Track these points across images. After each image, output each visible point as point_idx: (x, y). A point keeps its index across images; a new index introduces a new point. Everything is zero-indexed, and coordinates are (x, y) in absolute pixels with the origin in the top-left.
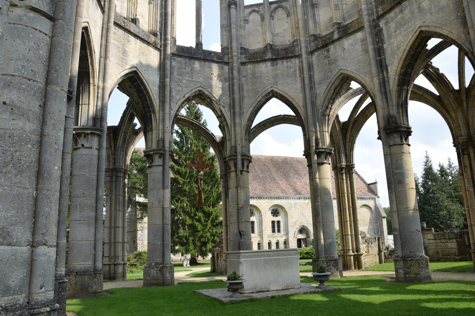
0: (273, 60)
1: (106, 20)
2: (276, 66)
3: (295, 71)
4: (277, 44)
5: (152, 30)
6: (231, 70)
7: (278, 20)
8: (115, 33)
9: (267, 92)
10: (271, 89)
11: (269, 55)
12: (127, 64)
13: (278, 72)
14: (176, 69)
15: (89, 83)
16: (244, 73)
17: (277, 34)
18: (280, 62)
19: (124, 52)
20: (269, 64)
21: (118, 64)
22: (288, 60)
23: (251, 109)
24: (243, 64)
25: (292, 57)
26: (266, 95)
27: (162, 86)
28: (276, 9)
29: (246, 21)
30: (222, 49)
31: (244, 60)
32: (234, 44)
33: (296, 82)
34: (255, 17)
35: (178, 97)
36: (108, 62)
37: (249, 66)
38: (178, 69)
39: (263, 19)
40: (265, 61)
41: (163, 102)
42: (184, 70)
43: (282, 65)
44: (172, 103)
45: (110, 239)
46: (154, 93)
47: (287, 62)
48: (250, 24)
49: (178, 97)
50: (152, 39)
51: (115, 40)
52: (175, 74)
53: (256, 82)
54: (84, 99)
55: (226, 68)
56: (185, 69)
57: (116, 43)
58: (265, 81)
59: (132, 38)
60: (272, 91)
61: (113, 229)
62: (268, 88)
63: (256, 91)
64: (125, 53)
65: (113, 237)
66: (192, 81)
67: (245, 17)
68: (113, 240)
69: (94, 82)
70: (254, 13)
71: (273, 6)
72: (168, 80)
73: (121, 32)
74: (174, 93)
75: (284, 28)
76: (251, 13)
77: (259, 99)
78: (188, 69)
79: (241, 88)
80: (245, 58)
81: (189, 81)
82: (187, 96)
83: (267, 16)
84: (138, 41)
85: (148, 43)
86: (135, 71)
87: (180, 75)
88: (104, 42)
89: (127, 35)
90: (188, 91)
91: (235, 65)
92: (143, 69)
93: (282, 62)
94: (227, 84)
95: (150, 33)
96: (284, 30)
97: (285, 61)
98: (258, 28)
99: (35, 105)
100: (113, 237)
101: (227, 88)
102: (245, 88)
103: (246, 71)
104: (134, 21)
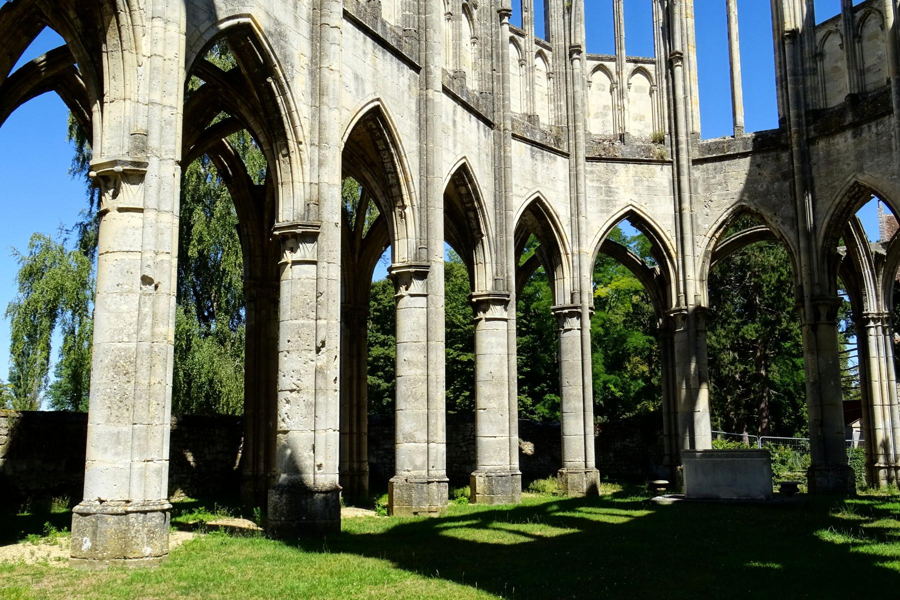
0: (856, 127)
1: (573, 164)
2: (861, 135)
3: (890, 140)
4: (869, 88)
5: (655, 134)
7: (869, 40)
8: (592, 172)
9: (847, 187)
10: (854, 180)
11: (849, 118)
12: (615, 206)
13: (865, 146)
14: (700, 182)
15: (560, 253)
16: (814, 159)
17: (869, 69)
18: (865, 126)
19: (609, 192)
20: (849, 134)
21: (602, 211)
22: (879, 121)
23: (826, 220)
24: (811, 141)
25: (883, 115)
26: (849, 191)
28: (863, 19)
30: (780, 122)
32: (792, 112)
33: (891, 160)
34: (834, 44)
35: (707, 226)
36: (582, 219)
37: (822, 144)
38: (704, 181)
39: (841, 46)
40: (842, 129)
42: (713, 181)
43: (870, 132)
44: (697, 238)
45: (670, 430)
46: (665, 231)
47: (877, 126)
48: (827, 59)
49: (707, 226)
50: (657, 150)
51: (593, 180)
52: (700, 190)
53: (832, 171)
54: (558, 274)
55: (785, 156)
56: (714, 177)
57: (595, 184)
58: (845, 166)
59: (619, 166)
60: (856, 182)
61: (672, 416)
62: (849, 178)
63: (832, 188)
64: (610, 192)
65: (673, 427)
66: (727, 195)
67: (816, 48)
68: (673, 432)
69: (566, 251)
70: (831, 36)
71: (858, 15)
72: (686, 205)
73: (601, 166)
74: (700, 221)
75: (880, 53)
76: (825, 38)
77: (837, 201)
78: (719, 177)
80: (815, 130)
81: (721, 195)
82: (721, 220)
84: (631, 166)
85: (649, 162)
86: (631, 210)
87: (707, 189)
88: (574, 195)
89: (611, 165)
90: (722, 212)
91: (795, 148)
92: (643, 204)
93: (869, 127)
94: (788, 184)
95: (654, 142)
96: (879, 58)
97: (873, 124)
98: (839, 64)
99: (421, 357)
100: (673, 427)
101: (788, 190)
103: (818, 155)
104: (622, 138)
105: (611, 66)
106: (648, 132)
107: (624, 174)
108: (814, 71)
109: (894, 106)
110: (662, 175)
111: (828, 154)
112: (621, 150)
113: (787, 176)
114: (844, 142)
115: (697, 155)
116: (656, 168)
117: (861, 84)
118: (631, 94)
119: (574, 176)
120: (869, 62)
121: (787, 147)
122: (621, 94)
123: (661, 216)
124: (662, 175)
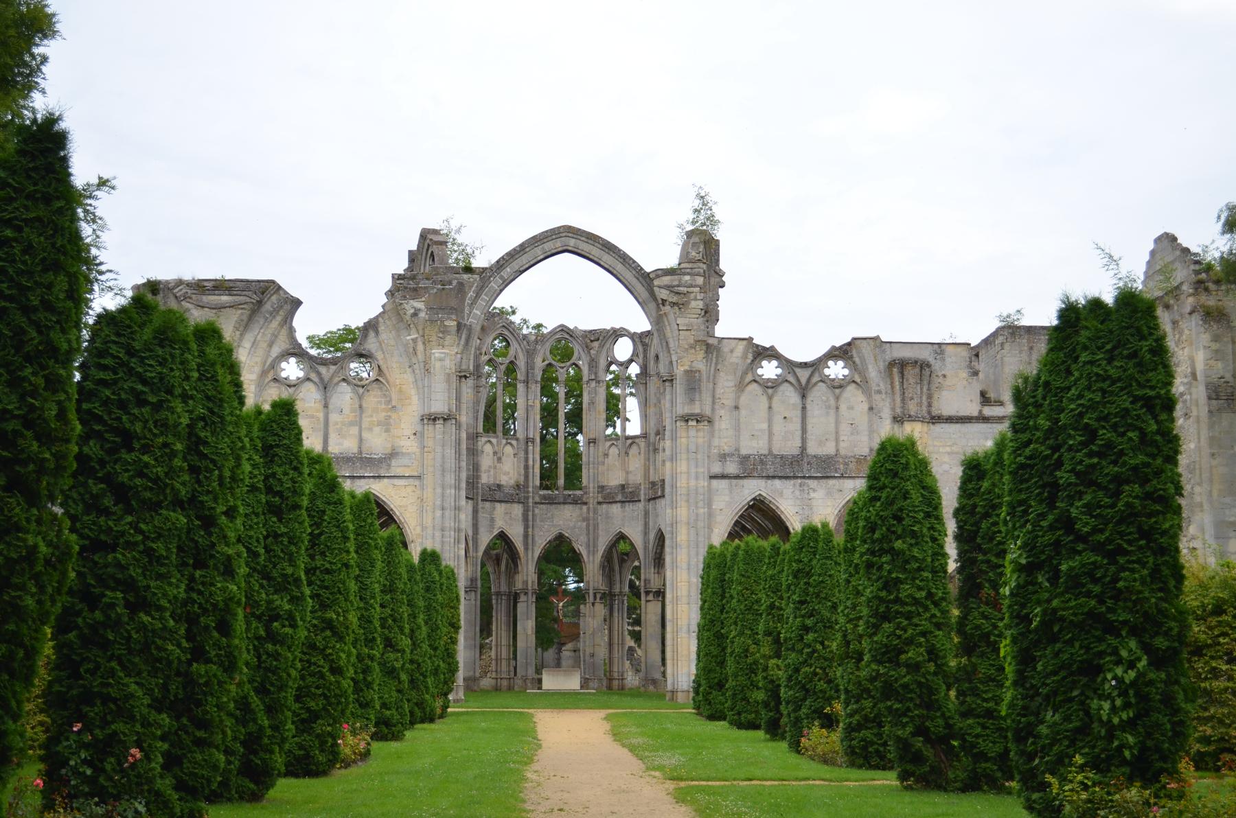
6: (588, 509)
19: (492, 520)
24: (599, 503)
27: (526, 536)
29: (606, 455)
31: (600, 499)
34: (614, 451)
37: (604, 506)
41: (526, 549)
43: (629, 507)
55: (585, 507)
71: (629, 441)
73: (488, 504)
79: (596, 527)
83: (623, 454)
102: (600, 527)
105: (494, 441)
106: (512, 482)
107: (500, 508)
108: (603, 463)
109: (642, 498)
110: (517, 510)
111: (607, 513)
112: (498, 495)
113: (586, 519)
114: (615, 509)
115: (537, 499)
116: (516, 505)
117: (627, 479)
118: (504, 459)
119: (475, 511)
120: (631, 468)
121: (586, 503)
122: (499, 459)
123: (516, 533)
124: (517, 510)
